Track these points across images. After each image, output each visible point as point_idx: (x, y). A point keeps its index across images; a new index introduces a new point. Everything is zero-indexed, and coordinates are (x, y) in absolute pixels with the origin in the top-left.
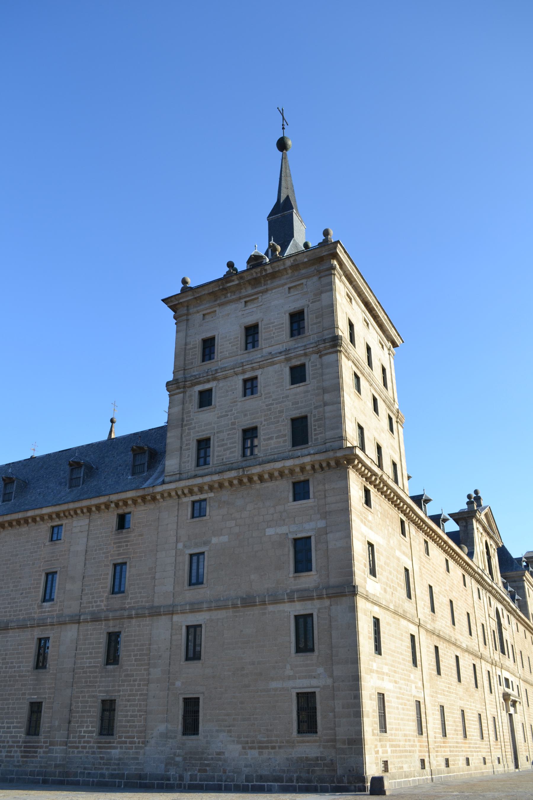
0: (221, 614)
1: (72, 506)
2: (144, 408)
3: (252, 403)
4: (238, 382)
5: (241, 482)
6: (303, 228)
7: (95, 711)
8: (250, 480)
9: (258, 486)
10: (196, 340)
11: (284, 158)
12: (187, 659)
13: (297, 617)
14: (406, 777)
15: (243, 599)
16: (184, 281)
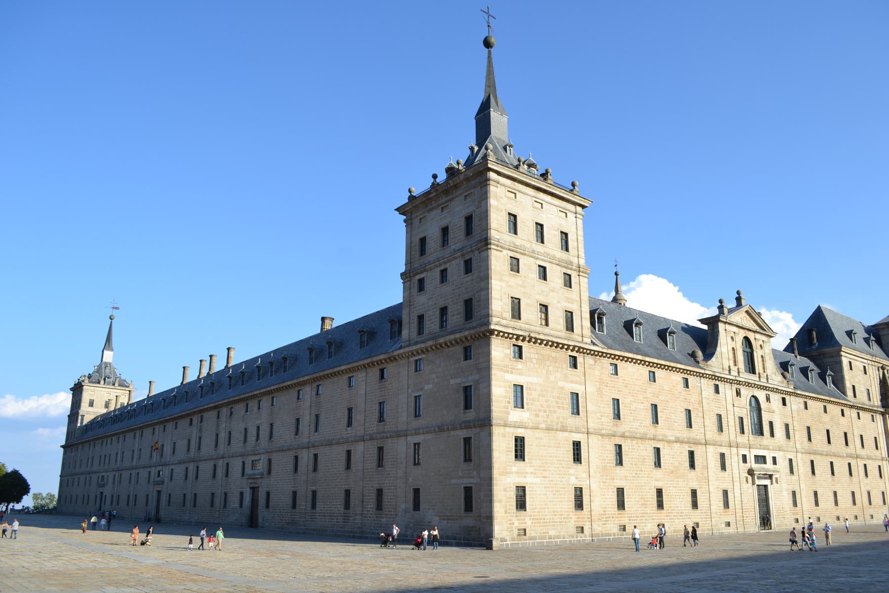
0: (429, 436)
1: (355, 364)
2: (390, 293)
3: (446, 289)
4: (437, 273)
5: (436, 346)
6: (505, 119)
7: (374, 496)
8: (441, 346)
9: (446, 350)
10: (416, 240)
11: (489, 57)
12: (415, 464)
13: (465, 439)
14: (550, 538)
15: (439, 427)
16: (410, 191)
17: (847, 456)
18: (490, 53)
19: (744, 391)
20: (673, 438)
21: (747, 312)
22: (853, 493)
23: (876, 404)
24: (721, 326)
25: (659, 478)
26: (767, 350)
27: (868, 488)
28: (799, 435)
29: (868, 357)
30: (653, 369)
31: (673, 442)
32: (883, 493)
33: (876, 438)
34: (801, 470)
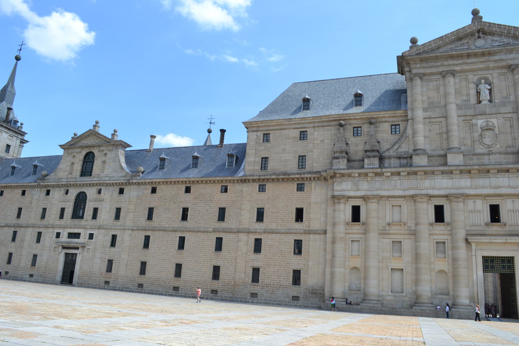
17: (215, 231)
18: (17, 63)
27: (256, 265)
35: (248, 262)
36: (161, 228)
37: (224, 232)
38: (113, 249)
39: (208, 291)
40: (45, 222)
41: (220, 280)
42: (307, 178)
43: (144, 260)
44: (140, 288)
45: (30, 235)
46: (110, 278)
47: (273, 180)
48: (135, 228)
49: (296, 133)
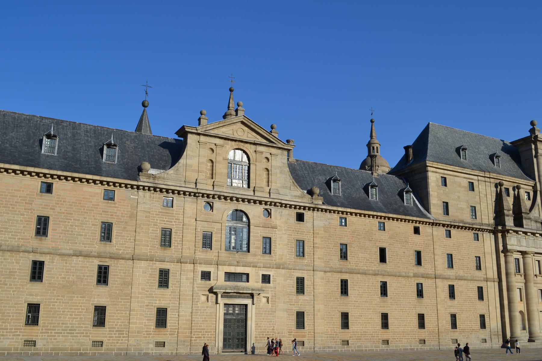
17: (415, 276)
19: (217, 204)
20: (71, 252)
21: (242, 123)
22: (421, 317)
23: (486, 221)
24: (191, 139)
25: (35, 292)
26: (279, 161)
27: (453, 311)
28: (323, 254)
29: (477, 173)
30: (50, 180)
31: (70, 255)
32: (482, 317)
33: (478, 258)
34: (320, 289)
35: (446, 308)
36: (361, 271)
37: (423, 277)
38: (301, 297)
39: (416, 341)
40: (173, 251)
41: (426, 329)
42: (482, 229)
43: (345, 311)
44: (346, 346)
45: (144, 275)
46: (304, 336)
47: (458, 227)
48: (328, 269)
49: (465, 183)
